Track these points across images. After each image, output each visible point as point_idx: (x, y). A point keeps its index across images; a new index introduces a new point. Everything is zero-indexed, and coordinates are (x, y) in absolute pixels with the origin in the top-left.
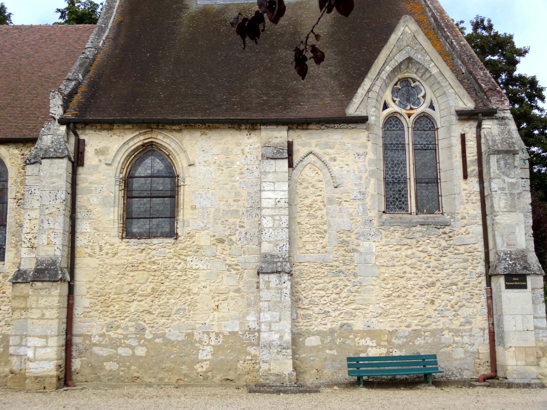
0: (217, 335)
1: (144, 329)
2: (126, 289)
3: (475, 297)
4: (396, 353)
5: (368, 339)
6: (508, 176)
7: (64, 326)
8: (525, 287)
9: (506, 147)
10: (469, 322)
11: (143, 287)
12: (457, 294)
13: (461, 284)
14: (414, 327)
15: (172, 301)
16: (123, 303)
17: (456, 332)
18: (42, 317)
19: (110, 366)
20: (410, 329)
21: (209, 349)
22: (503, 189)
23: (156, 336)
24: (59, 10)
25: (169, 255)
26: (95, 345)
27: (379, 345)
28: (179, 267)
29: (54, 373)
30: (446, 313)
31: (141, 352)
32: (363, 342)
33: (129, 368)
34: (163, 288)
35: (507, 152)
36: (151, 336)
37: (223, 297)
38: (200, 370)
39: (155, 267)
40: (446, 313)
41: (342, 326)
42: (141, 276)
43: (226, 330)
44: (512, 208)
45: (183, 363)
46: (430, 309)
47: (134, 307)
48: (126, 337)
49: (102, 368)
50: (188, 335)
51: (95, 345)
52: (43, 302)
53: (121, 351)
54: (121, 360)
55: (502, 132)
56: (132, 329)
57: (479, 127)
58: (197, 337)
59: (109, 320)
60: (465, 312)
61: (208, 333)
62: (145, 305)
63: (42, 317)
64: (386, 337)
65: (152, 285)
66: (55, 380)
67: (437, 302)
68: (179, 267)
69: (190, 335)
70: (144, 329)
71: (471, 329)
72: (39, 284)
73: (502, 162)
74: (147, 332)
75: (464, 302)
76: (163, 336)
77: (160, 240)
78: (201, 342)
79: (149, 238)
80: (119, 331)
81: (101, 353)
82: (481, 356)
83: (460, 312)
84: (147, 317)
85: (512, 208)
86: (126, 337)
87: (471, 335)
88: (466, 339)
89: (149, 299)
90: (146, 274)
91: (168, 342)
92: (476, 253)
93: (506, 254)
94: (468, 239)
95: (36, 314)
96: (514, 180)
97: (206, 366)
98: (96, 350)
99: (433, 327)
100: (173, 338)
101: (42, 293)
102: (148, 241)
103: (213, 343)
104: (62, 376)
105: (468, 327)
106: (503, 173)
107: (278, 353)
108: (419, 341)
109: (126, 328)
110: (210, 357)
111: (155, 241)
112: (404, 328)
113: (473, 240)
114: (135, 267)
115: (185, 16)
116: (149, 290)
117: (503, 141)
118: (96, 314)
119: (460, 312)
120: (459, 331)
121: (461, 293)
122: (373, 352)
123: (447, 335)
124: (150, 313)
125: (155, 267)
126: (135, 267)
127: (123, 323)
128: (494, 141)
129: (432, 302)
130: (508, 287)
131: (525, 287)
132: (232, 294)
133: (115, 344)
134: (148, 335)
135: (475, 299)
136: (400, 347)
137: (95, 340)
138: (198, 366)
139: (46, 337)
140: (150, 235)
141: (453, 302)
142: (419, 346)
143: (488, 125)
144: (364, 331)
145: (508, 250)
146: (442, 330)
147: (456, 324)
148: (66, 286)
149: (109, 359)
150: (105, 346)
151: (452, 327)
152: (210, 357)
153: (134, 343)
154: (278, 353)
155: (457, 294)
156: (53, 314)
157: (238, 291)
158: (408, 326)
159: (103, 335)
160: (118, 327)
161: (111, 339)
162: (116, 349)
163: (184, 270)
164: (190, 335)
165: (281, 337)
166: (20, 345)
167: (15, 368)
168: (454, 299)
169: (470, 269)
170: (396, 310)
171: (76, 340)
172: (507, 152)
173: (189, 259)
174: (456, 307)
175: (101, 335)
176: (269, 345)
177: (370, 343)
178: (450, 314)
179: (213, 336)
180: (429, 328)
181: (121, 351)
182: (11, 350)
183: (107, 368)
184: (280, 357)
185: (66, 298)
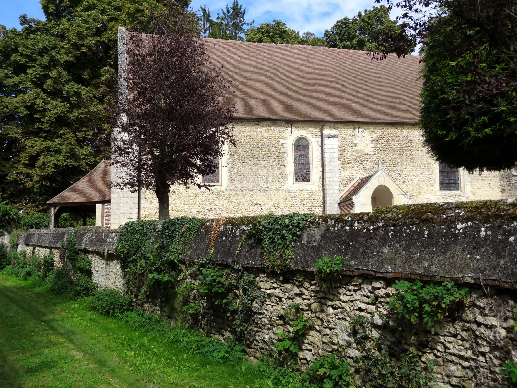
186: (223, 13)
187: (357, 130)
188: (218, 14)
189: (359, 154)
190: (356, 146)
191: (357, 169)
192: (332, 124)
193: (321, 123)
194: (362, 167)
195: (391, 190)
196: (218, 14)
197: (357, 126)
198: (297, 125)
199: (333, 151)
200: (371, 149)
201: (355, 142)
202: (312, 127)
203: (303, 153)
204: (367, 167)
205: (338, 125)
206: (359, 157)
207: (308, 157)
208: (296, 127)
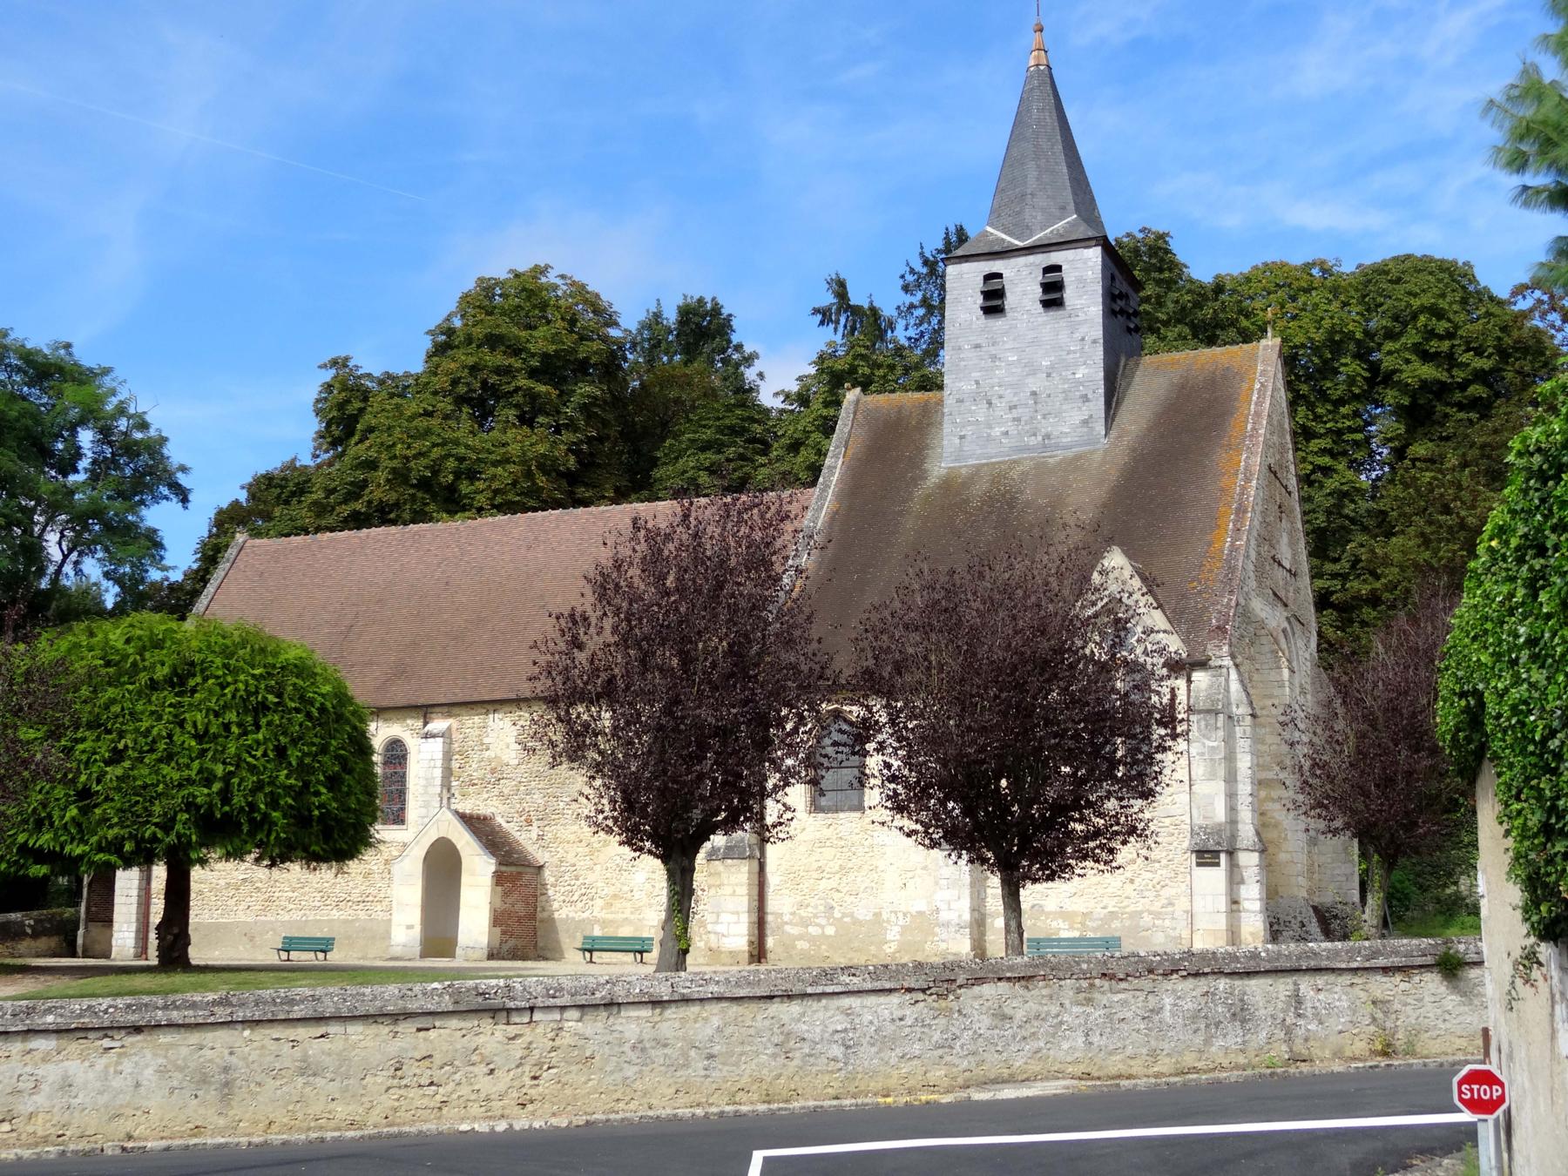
0: (905, 915)
1: (832, 908)
2: (815, 865)
3: (1180, 876)
4: (1090, 935)
5: (1060, 921)
6: (1208, 739)
7: (756, 903)
8: (1218, 864)
9: (1208, 706)
10: (1171, 904)
11: (831, 864)
12: (1159, 872)
13: (1164, 862)
14: (1110, 909)
15: (859, 879)
16: (812, 881)
17: (1157, 915)
18: (733, 894)
19: (801, 945)
20: (1106, 911)
21: (897, 929)
22: (1202, 754)
23: (844, 915)
24: (816, 311)
25: (857, 831)
26: (786, 923)
27: (1071, 928)
28: (866, 843)
29: (746, 948)
30: (1146, 894)
31: (830, 931)
32: (1054, 924)
33: (819, 947)
34: (850, 865)
35: (1208, 711)
36: (839, 915)
37: (910, 874)
38: (888, 951)
39: (842, 843)
40: (1146, 894)
41: (1033, 907)
42: (828, 853)
43: (913, 910)
44: (1211, 776)
45: (872, 943)
46: (1129, 888)
47: (824, 884)
48: (816, 916)
49: (794, 947)
50: (875, 914)
51: (786, 923)
52: (733, 879)
53: (811, 929)
54: (812, 940)
55: (1211, 686)
56: (822, 908)
57: (1189, 681)
58: (885, 916)
59: (799, 898)
60: (1166, 893)
61: (896, 913)
62: (833, 883)
63: (733, 894)
64: (1079, 920)
65: (840, 862)
66: (747, 955)
67: (1137, 881)
68: (866, 843)
69: (878, 915)
70: (832, 908)
71: (1173, 912)
72: (729, 861)
73: (1203, 723)
74: (836, 911)
75: (1167, 881)
76: (852, 915)
77: (847, 814)
78: (888, 921)
79: (837, 811)
80: (810, 909)
81: (792, 931)
82: (1183, 942)
83: (1161, 893)
84: (837, 896)
85: (1211, 776)
86: (816, 916)
87: (1173, 918)
88: (1167, 923)
89: (838, 876)
90: (833, 851)
91: (856, 922)
92: (1183, 826)
93: (1200, 828)
94: (1173, 810)
95: (728, 890)
96: (1215, 744)
97: (894, 946)
98: (788, 928)
99: (1132, 908)
100: (861, 918)
101: (733, 870)
102: (835, 815)
103: (900, 923)
104: (755, 952)
105: (1170, 909)
106: (1204, 736)
107: (956, 932)
108: (1116, 924)
109: (816, 907)
110: (898, 937)
111: (841, 815)
112: (1099, 910)
113: (1180, 811)
114: (822, 843)
115: (919, 493)
116: (837, 868)
117: (1208, 697)
118: (787, 892)
119: (1161, 893)
120: (1160, 913)
121: (1164, 872)
122: (1064, 934)
123: (1147, 918)
124: (838, 891)
125: (842, 843)
126: (822, 843)
127: (813, 902)
128: (1197, 698)
129: (1132, 881)
130: (1199, 864)
131: (1218, 864)
132: (919, 871)
133: (805, 923)
134: (837, 915)
135: (1180, 877)
136: (1095, 930)
137: (786, 918)
138: (885, 947)
139: (738, 913)
140: (837, 809)
141: (1155, 881)
142: (1116, 930)
143: (1199, 677)
144: (1055, 913)
145: (1203, 823)
146: (1141, 912)
147: (1156, 907)
148: (755, 864)
149: (801, 937)
150: (796, 925)
151: (1152, 909)
152: (898, 937)
153: (823, 921)
154: (956, 932)
155: (1159, 872)
156: (744, 890)
157: (925, 868)
158: (1104, 908)
159: (793, 914)
160: (807, 906)
161: (802, 918)
162: (807, 926)
163: (872, 846)
164: (878, 915)
165: (960, 916)
166: (716, 923)
167: (714, 945)
168: (1157, 878)
169: (1175, 844)
170: (1092, 890)
171: (770, 918)
172: (1208, 711)
173: (875, 834)
174: (1158, 887)
175: (792, 914)
176: (947, 925)
177: (1062, 925)
178: (1151, 894)
179: (900, 915)
180: (1127, 910)
181: (811, 929)
182: (710, 927)
183: (799, 947)
184: (958, 936)
185: (756, 876)
186: (912, 271)
187: (491, 716)
188: (903, 277)
189: (493, 765)
190: (487, 749)
191: (486, 796)
192: (445, 709)
193: (425, 711)
194: (496, 792)
195: (459, 847)
196: (903, 277)
197: (490, 707)
198: (386, 716)
199: (432, 763)
200: (513, 754)
201: (486, 741)
202: (413, 717)
203: (398, 770)
204: (506, 791)
205: (456, 710)
206: (493, 771)
207: (404, 776)
208: (386, 720)
